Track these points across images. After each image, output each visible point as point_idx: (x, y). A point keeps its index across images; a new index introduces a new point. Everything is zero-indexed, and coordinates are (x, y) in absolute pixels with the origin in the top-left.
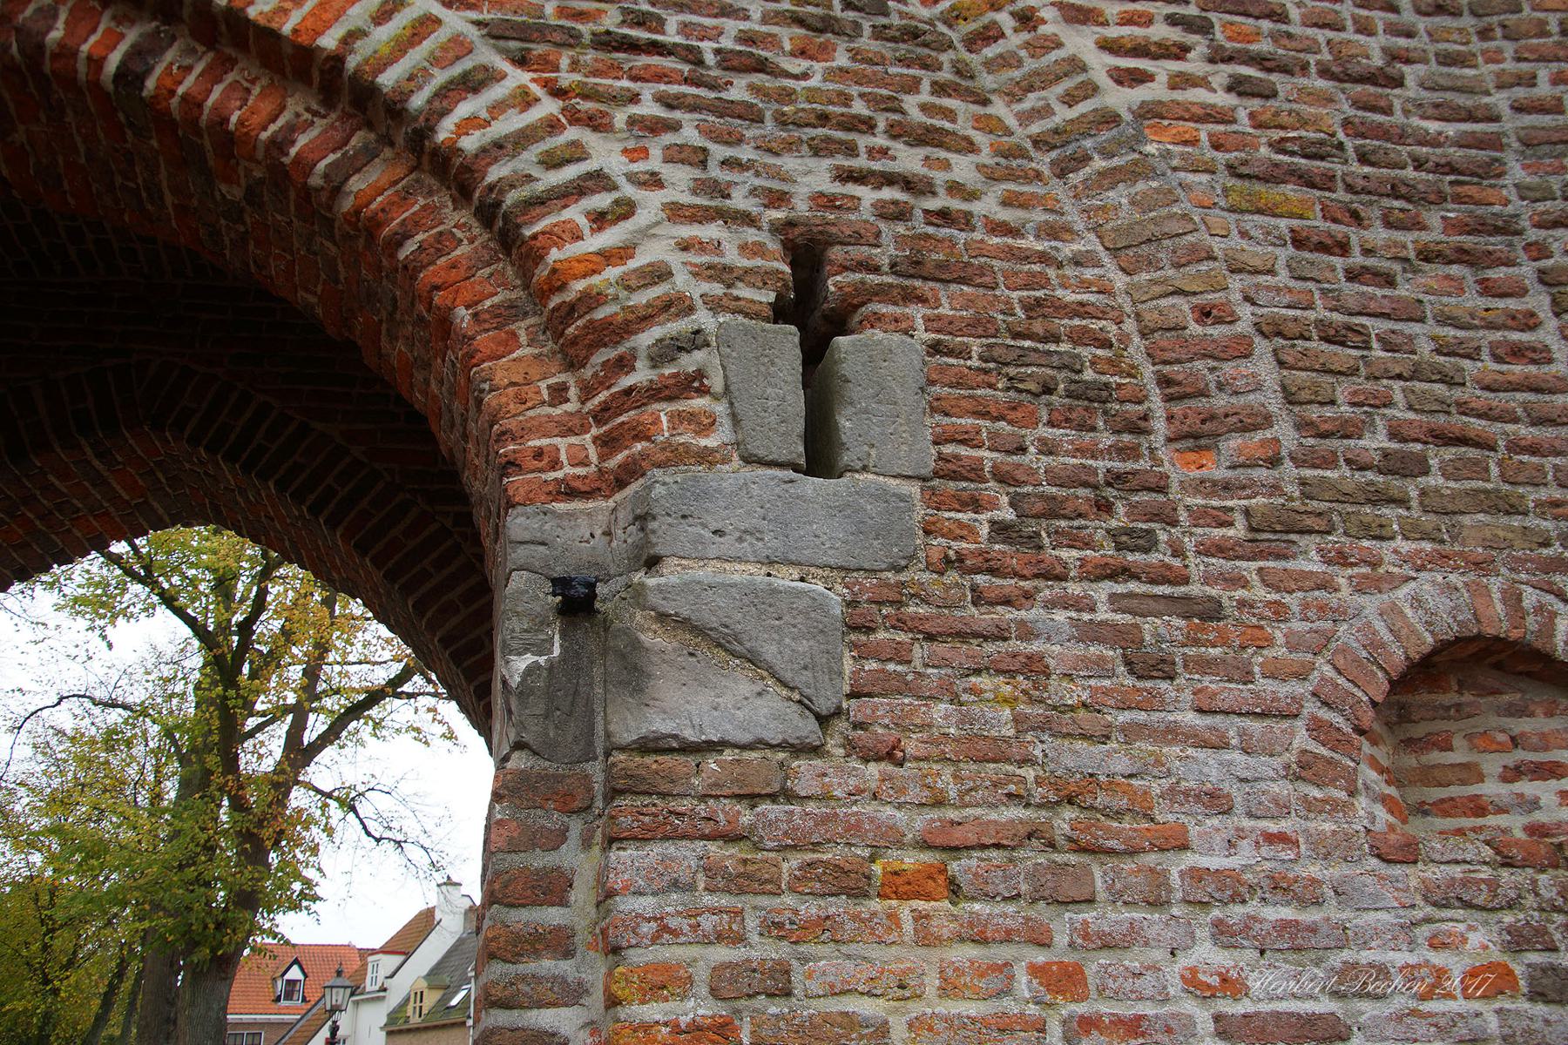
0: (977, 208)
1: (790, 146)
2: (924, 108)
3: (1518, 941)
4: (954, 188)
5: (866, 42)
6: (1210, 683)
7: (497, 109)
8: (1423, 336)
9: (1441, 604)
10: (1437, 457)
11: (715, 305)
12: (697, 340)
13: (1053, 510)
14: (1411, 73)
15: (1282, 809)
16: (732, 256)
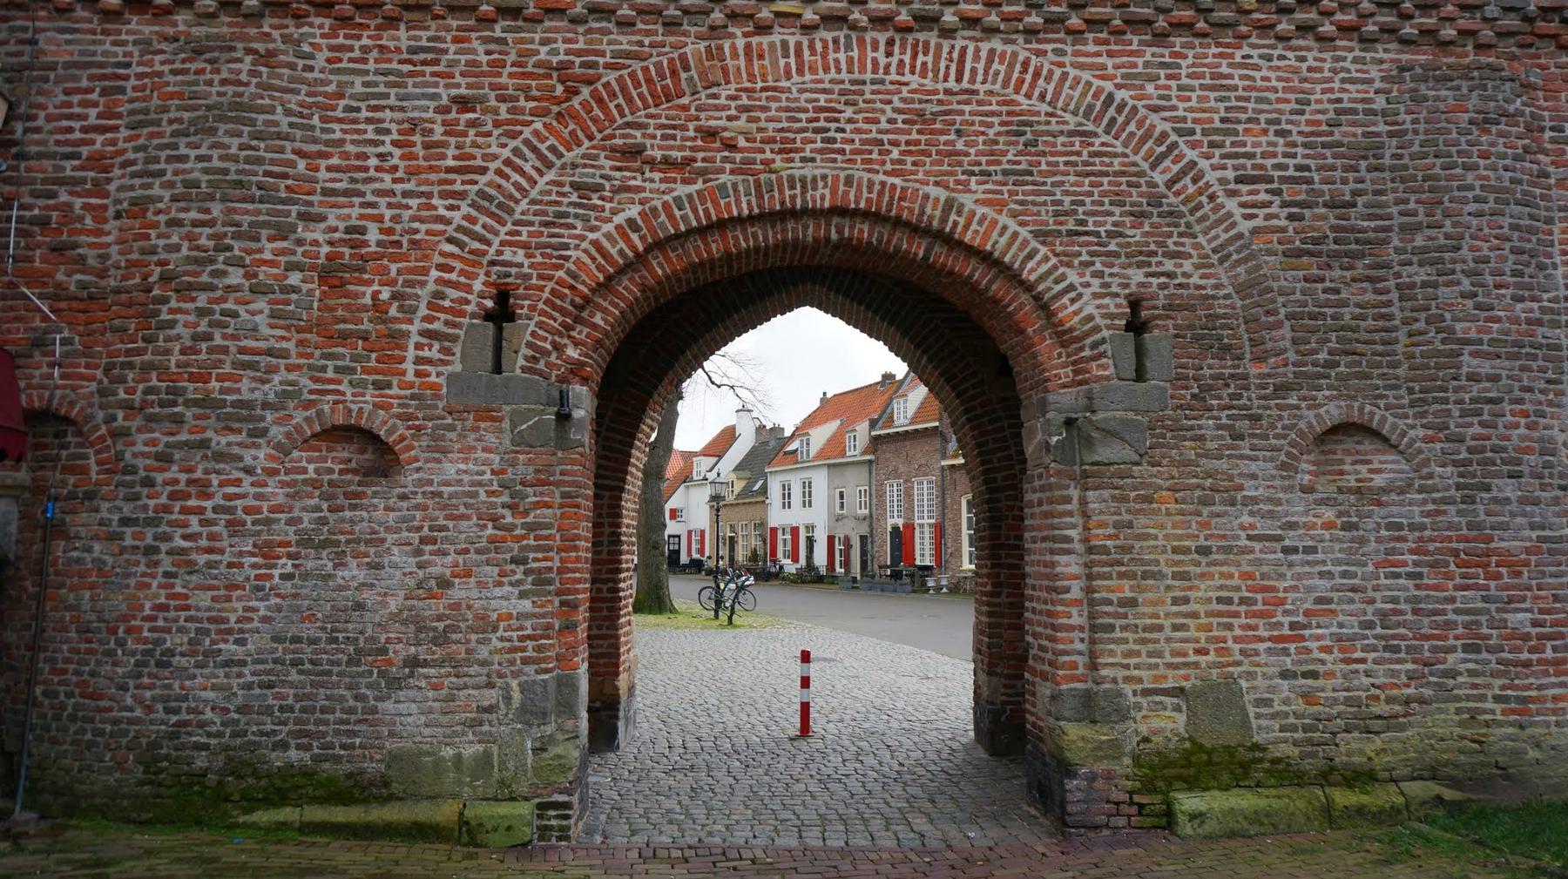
0: (1191, 281)
1: (1130, 265)
2: (1175, 244)
3: (1340, 514)
4: (1185, 275)
5: (1155, 219)
6: (1255, 441)
7: (1039, 264)
9: (1335, 412)
10: (1344, 360)
11: (1108, 327)
12: (1103, 341)
13: (1211, 388)
14: (1360, 200)
15: (1274, 477)
16: (1113, 310)
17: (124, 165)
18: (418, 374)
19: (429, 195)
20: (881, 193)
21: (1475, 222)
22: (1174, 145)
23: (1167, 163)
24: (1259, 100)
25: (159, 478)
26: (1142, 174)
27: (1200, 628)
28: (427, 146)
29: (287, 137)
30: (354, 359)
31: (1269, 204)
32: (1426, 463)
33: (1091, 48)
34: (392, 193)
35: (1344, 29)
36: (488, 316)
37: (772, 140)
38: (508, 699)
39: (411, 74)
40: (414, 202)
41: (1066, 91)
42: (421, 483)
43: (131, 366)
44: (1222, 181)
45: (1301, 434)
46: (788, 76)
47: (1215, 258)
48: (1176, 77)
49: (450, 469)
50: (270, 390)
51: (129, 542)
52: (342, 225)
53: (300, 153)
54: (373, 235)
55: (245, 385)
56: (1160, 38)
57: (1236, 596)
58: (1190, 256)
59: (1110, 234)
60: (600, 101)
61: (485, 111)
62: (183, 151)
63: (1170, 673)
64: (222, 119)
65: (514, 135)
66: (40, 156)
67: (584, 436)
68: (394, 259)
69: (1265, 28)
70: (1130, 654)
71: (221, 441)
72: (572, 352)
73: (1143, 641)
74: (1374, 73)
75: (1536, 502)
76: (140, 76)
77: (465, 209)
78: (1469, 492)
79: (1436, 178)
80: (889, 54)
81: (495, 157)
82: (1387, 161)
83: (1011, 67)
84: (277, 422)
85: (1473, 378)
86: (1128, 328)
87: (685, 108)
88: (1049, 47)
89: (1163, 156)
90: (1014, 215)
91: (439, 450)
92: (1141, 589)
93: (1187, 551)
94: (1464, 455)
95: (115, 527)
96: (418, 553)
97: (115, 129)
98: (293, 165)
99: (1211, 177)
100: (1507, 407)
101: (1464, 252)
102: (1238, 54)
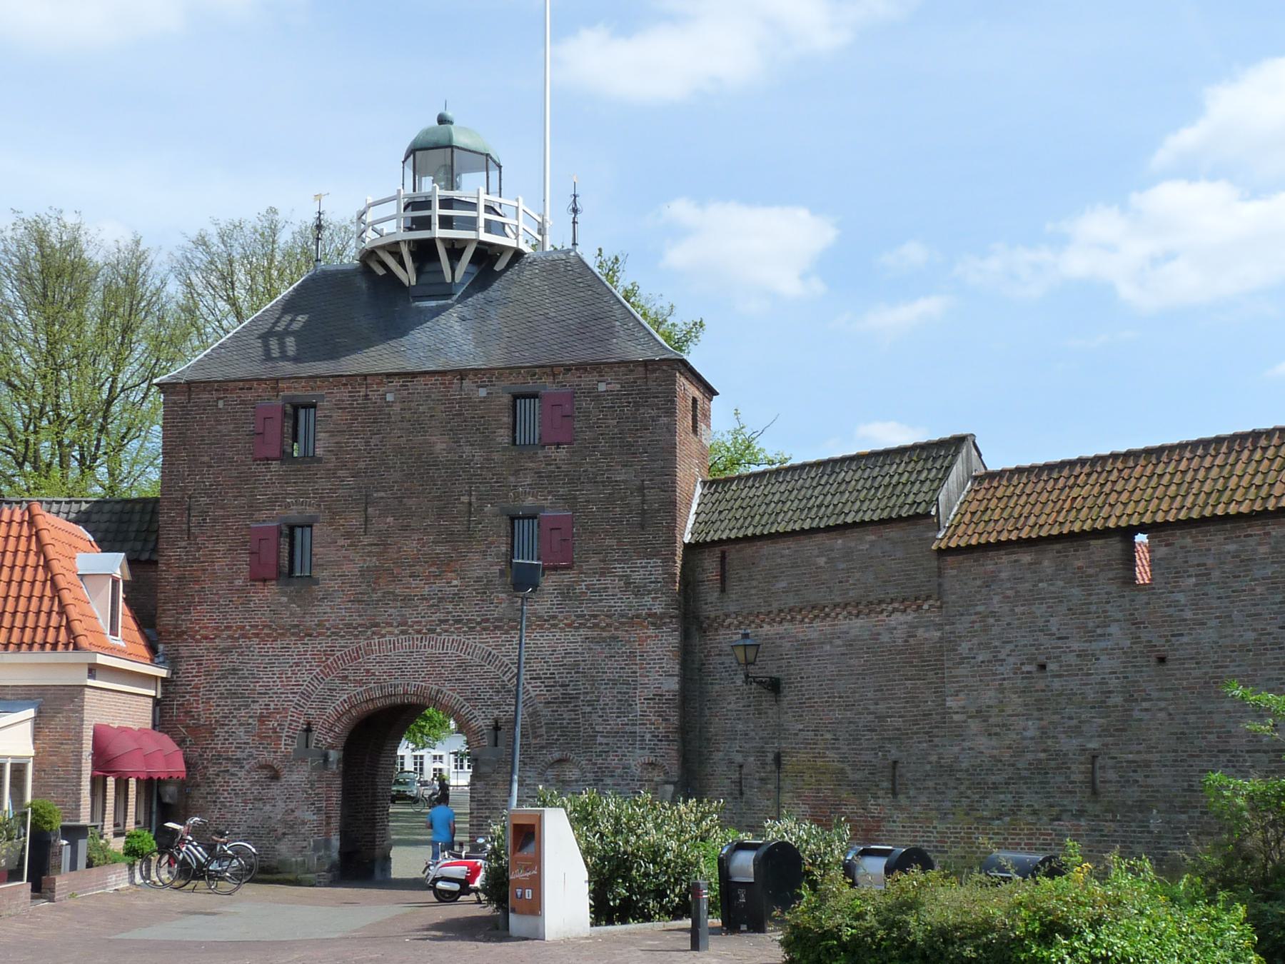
10: (562, 738)
14: (572, 684)
17: (204, 687)
21: (605, 691)
22: (510, 668)
23: (508, 674)
25: (216, 780)
28: (287, 678)
31: (540, 687)
32: (585, 772)
33: (485, 636)
34: (276, 693)
37: (385, 672)
38: (310, 844)
40: (283, 696)
41: (476, 651)
42: (286, 781)
44: (526, 679)
45: (546, 763)
49: (295, 777)
50: (244, 755)
52: (263, 704)
54: (272, 706)
55: (238, 753)
59: (488, 699)
65: (311, 673)
66: (181, 685)
68: (278, 713)
69: (541, 627)
72: (329, 740)
75: (619, 785)
76: (207, 660)
77: (298, 698)
82: (581, 670)
85: (600, 744)
86: (494, 728)
87: (361, 663)
89: (506, 672)
90: (458, 693)
92: (492, 813)
95: (205, 795)
96: (285, 802)
97: (200, 676)
98: (249, 686)
100: (611, 754)
101: (601, 702)
102: (533, 635)
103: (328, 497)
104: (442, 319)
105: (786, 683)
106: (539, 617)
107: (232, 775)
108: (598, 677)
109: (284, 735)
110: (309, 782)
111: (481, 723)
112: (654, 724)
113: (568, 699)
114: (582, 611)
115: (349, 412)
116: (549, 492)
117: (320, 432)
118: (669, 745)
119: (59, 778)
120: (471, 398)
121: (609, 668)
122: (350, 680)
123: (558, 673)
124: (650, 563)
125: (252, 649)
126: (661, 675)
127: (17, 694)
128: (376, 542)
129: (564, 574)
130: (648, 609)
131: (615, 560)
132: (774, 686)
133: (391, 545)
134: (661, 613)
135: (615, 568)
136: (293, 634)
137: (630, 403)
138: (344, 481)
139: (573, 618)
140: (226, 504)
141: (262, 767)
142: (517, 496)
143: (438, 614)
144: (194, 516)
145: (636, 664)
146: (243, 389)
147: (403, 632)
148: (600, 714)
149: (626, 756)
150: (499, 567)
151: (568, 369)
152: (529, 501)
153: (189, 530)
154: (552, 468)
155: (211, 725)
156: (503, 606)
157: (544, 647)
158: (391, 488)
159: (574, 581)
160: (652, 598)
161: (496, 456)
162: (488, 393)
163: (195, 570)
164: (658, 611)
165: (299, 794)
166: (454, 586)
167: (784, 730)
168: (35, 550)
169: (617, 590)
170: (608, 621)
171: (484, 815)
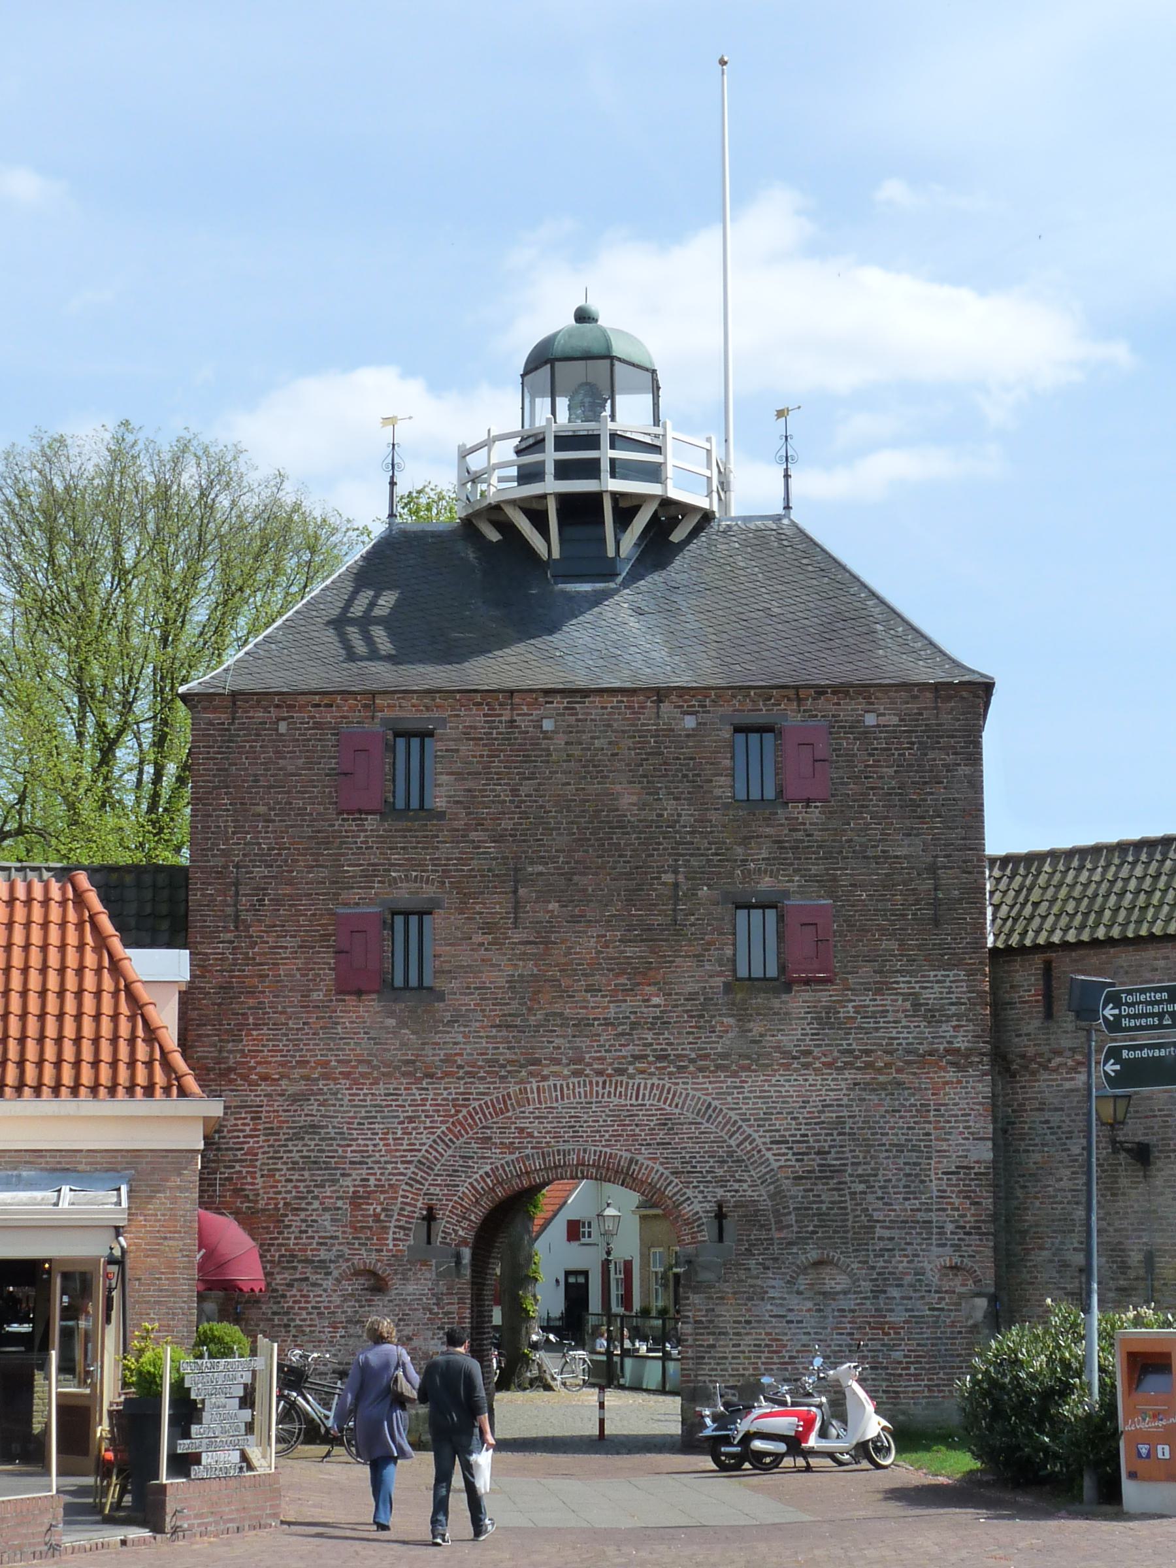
3: (815, 1305)
8: (824, 1206)
9: (815, 1256)
10: (820, 1230)
14: (833, 1150)
17: (264, 1153)
18: (394, 1245)
19: (396, 1163)
20: (600, 1156)
21: (885, 1161)
22: (740, 1127)
23: (737, 1135)
24: (783, 1102)
25: (288, 1294)
26: (725, 1141)
27: (745, 1358)
28: (394, 1139)
29: (334, 1139)
30: (367, 1239)
32: (858, 1280)
33: (701, 1080)
34: (379, 1162)
35: (828, 1065)
36: (424, 1219)
37: (550, 1132)
39: (387, 1106)
40: (389, 1166)
41: (688, 1102)
43: (273, 1245)
44: (764, 1143)
45: (798, 1267)
46: (557, 1101)
47: (759, 1182)
48: (743, 1093)
49: (411, 1288)
51: (276, 1322)
53: (338, 1145)
54: (372, 1182)
55: (322, 1253)
56: (735, 1074)
57: (763, 1343)
58: (746, 1181)
59: (707, 1172)
60: (471, 1116)
61: (420, 1122)
62: (290, 1148)
63: (731, 1379)
64: (306, 1133)
65: (433, 1133)
66: (227, 1149)
67: (467, 1272)
68: (382, 1192)
69: (787, 1067)
70: (713, 1370)
71: (313, 1278)
72: (461, 1233)
73: (718, 1364)
74: (844, 1086)
77: (413, 1169)
78: (877, 1293)
79: (868, 1139)
80: (604, 1088)
81: (424, 1144)
82: (847, 1130)
83: (661, 1093)
84: (337, 1268)
85: (880, 1239)
86: (717, 1216)
87: (510, 1118)
88: (680, 1081)
89: (735, 1132)
90: (662, 1164)
91: (405, 1279)
92: (717, 1340)
93: (739, 1322)
94: (875, 1276)
95: (269, 1316)
97: (257, 1136)
98: (337, 1151)
99: (759, 1141)
100: (897, 1253)
101: (880, 1177)
102: (774, 1079)
103: (457, 870)
104: (607, 609)
105: (1160, 1151)
106: (784, 1052)
107: (314, 1285)
108: (875, 1140)
109: (392, 1225)
110: (433, 1295)
111: (697, 1207)
112: (958, 1209)
113: (828, 1173)
114: (850, 1045)
115: (485, 745)
116: (795, 871)
117: (441, 773)
118: (981, 1240)
119: (161, 1291)
120: (673, 730)
121: (892, 1128)
122: (496, 1144)
123: (813, 1135)
124: (948, 976)
125: (340, 1096)
126: (968, 1139)
127: (97, 1163)
128: (532, 939)
129: (822, 990)
130: (948, 1042)
131: (897, 971)
132: (1142, 1155)
133: (555, 943)
134: (966, 1049)
135: (897, 983)
136: (404, 1074)
137: (913, 743)
138: (479, 848)
139: (836, 1054)
140: (295, 877)
141: (357, 1273)
142: (747, 874)
143: (631, 1047)
144: (244, 895)
145: (930, 1122)
146: (318, 706)
147: (576, 1074)
148: (880, 1194)
149: (918, 1256)
150: (723, 979)
151: (820, 691)
152: (766, 883)
153: (237, 916)
154: (799, 835)
155: (279, 1209)
156: (730, 1035)
157: (792, 1097)
158: (554, 860)
159: (834, 1001)
160: (954, 1027)
161: (714, 816)
162: (699, 724)
163: (247, 977)
164: (963, 1046)
165: (420, 1314)
166: (655, 1006)
167: (1160, 1218)
168: (92, 944)
169: (901, 1015)
170: (887, 1058)
171: (705, 1343)
